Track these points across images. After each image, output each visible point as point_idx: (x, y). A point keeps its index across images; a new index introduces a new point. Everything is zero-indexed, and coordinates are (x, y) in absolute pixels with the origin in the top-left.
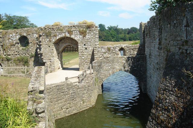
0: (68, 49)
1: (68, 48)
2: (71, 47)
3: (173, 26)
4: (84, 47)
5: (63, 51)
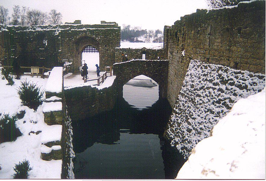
2: (92, 47)
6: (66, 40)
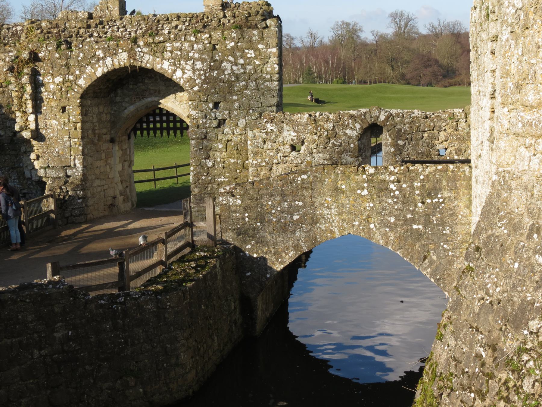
0: (161, 122)
5: (135, 130)
6: (54, 82)
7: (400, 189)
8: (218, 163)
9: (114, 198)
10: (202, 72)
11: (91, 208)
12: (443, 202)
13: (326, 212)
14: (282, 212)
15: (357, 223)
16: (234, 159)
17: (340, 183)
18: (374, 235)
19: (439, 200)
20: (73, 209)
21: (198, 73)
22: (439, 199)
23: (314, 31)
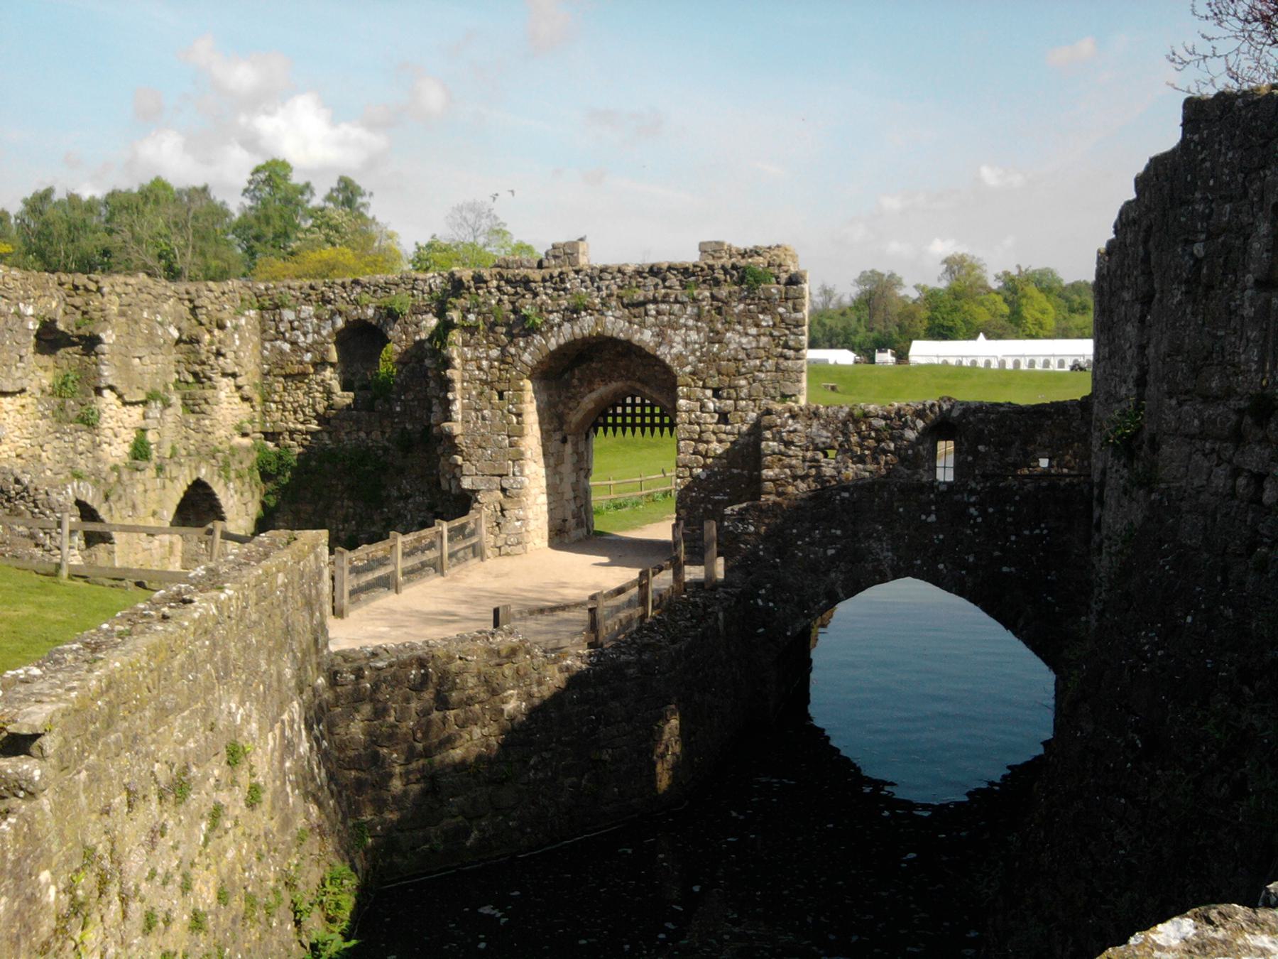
1: (624, 406)
2: (638, 400)
3: (1187, 282)
4: (711, 405)
7: (983, 513)
8: (715, 474)
9: (565, 521)
10: (697, 346)
11: (533, 534)
12: (1047, 535)
13: (874, 545)
14: (812, 544)
15: (919, 562)
16: (737, 468)
17: (896, 504)
18: (943, 579)
19: (1042, 531)
20: (508, 535)
21: (690, 347)
22: (1042, 530)
23: (829, 286)
